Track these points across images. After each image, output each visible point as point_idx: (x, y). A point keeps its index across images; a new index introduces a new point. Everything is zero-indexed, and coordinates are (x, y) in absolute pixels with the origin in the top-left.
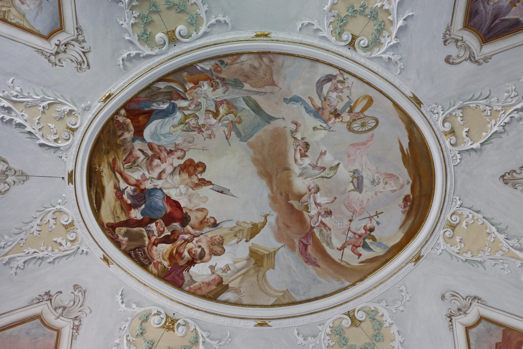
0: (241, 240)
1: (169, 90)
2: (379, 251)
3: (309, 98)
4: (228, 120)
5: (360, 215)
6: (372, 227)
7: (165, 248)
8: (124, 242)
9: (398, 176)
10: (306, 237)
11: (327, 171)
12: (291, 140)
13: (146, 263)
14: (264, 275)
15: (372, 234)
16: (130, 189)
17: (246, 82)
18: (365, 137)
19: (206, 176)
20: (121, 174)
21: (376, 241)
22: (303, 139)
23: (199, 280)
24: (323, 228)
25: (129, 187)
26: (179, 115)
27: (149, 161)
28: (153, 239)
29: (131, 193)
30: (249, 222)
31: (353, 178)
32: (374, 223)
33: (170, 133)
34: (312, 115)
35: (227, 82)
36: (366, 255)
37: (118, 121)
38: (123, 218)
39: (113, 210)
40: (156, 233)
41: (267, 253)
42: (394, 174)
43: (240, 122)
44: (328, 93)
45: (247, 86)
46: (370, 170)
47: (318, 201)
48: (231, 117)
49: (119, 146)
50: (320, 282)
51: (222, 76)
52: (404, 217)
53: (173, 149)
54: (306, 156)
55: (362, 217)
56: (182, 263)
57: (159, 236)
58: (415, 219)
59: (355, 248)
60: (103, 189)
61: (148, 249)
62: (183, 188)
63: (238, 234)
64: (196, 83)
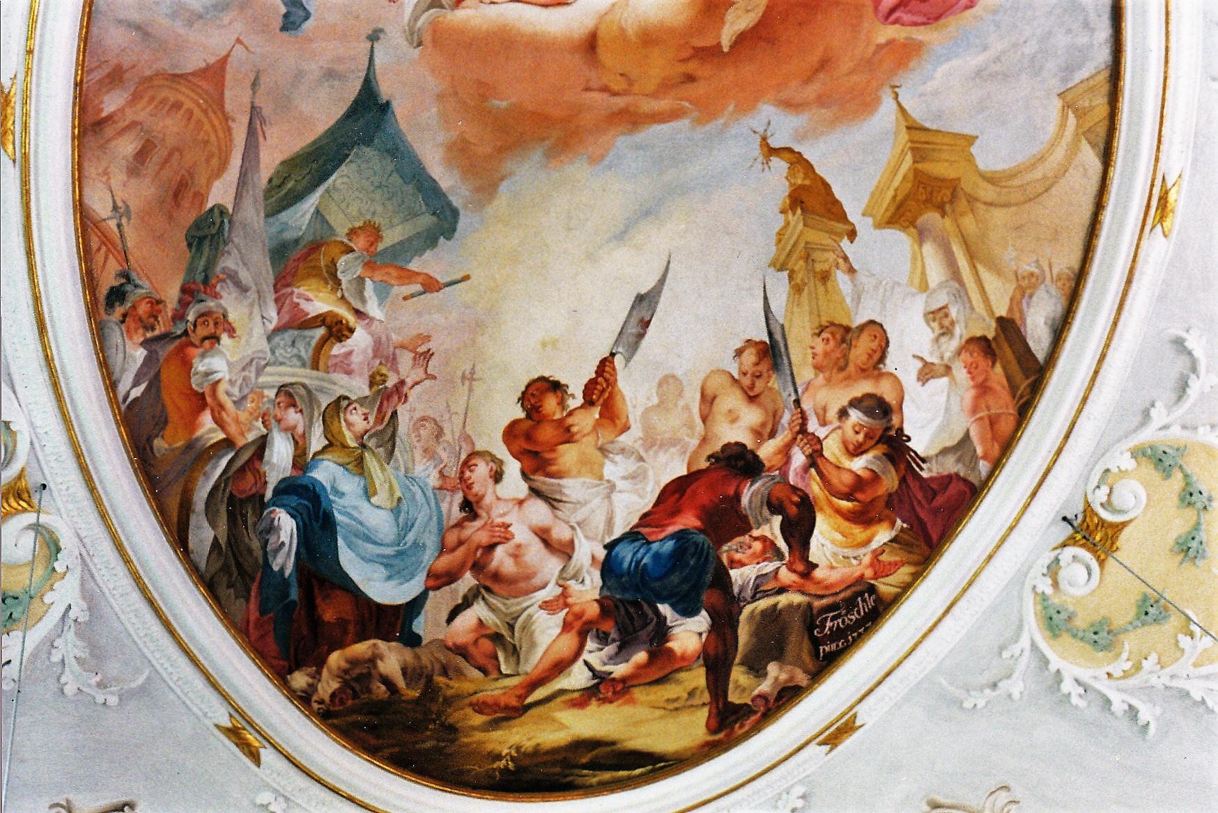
0: (846, 258)
1: (223, 509)
4: (361, 280)
7: (826, 540)
8: (783, 677)
13: (871, 603)
14: (992, 179)
16: (595, 654)
17: (201, 197)
20: (534, 685)
23: (962, 423)
25: (585, 656)
26: (326, 473)
27: (495, 587)
28: (786, 576)
29: (610, 649)
30: (780, 221)
33: (396, 511)
35: (199, 277)
37: (333, 695)
38: (697, 678)
39: (662, 712)
40: (769, 567)
41: (909, 159)
43: (374, 232)
45: (220, 193)
48: (348, 268)
49: (431, 690)
51: (172, 294)
53: (459, 497)
56: (890, 481)
57: (779, 555)
60: (581, 745)
61: (822, 597)
62: (614, 469)
63: (818, 267)
64: (199, 402)
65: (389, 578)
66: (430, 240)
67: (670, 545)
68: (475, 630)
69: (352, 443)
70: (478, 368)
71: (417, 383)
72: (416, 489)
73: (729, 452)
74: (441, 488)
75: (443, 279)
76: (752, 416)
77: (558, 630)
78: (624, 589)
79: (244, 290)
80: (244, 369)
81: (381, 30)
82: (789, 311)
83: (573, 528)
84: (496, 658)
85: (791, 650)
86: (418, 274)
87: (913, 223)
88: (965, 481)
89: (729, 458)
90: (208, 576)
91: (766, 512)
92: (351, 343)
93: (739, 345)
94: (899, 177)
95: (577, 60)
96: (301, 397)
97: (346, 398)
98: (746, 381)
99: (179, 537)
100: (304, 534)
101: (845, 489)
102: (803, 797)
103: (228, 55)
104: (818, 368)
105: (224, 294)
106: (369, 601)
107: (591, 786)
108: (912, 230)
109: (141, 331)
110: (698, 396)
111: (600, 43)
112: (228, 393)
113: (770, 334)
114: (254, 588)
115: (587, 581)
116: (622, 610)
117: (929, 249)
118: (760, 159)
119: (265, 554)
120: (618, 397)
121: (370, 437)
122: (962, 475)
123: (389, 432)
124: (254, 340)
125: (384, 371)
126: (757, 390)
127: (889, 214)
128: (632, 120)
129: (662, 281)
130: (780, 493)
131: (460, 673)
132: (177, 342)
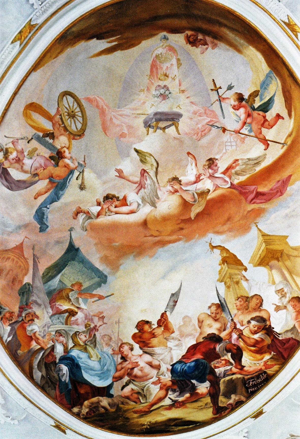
0: (244, 277)
1: (43, 367)
2: (275, 88)
3: (35, 198)
4: (77, 299)
5: (216, 116)
6: (236, 97)
8: (237, 398)
9: (154, 55)
12: (103, 220)
13: (265, 376)
15: (246, 97)
16: (172, 395)
17: (21, 281)
18: (90, 111)
19: (154, 319)
21: (259, 91)
22: (99, 204)
24: (233, 171)
25: (169, 396)
26: (75, 353)
27: (135, 379)
29: (177, 394)
30: (219, 268)
31: (158, 128)
33: (100, 361)
34: (61, 192)
35: (24, 304)
36: (279, 107)
37: (87, 413)
39: (197, 410)
40: (228, 368)
41: (264, 245)
42: (151, 62)
43: (80, 285)
44: (26, 172)
45: (27, 279)
46: (144, 103)
47: (193, 179)
48: (73, 296)
49: (119, 409)
51: (16, 310)
52: (222, 45)
53: (120, 356)
54: (125, 198)
55: (219, 112)
56: (268, 341)
57: (231, 364)
58: (226, 26)
59: (267, 123)
60: (170, 420)
61: (248, 375)
62: (171, 344)
63: (235, 280)
64: (31, 338)
65: (100, 380)
66: (99, 285)
67: (193, 364)
68: (131, 391)
69: (82, 344)
70: (120, 320)
71: (101, 326)
72: (105, 355)
73: (210, 336)
74: (113, 354)
75: (105, 295)
76: (217, 325)
77: (159, 390)
78: (179, 377)
79: (40, 305)
80: (43, 327)
81: (73, 228)
82: (226, 294)
83: (159, 361)
84: (139, 398)
85: (239, 391)
86: (96, 295)
87: (267, 264)
88: (295, 340)
89: (210, 338)
90: (42, 385)
91: (225, 352)
92: (77, 317)
93: (209, 305)
94: (261, 251)
95: (141, 229)
96: (63, 333)
97: (78, 332)
98: (213, 315)
99: (30, 376)
100: (71, 370)
101: (252, 344)
102: (247, 432)
103: (23, 242)
104: (238, 309)
105: (33, 307)
106: (95, 387)
107: (175, 431)
108: (268, 267)
109: (8, 322)
110: (197, 321)
111: (148, 222)
112: (39, 335)
113: (220, 301)
114: (57, 386)
115: (166, 375)
116: (180, 383)
117: (274, 271)
118: (210, 250)
119: (59, 377)
120: (169, 324)
121: (88, 341)
122: (294, 338)
123: (94, 340)
124: (46, 318)
125: (89, 323)
126: (217, 318)
127: (258, 262)
128: (163, 243)
129: (180, 289)
130: (228, 346)
131: (127, 403)
132: (20, 323)
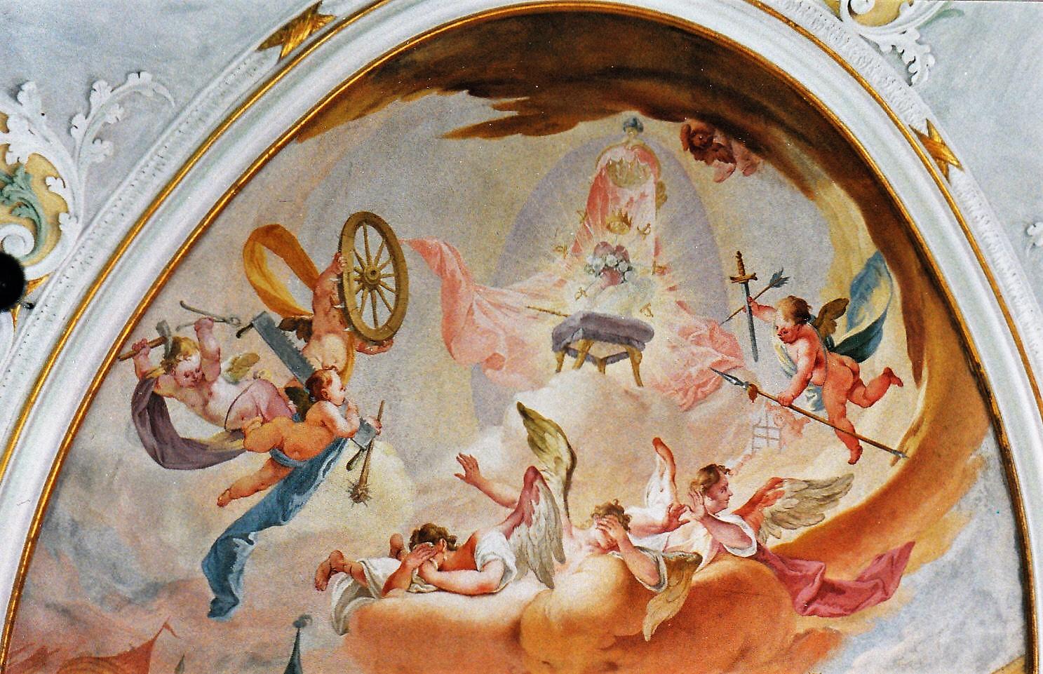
2: (885, 300)
3: (221, 505)
5: (735, 351)
6: (786, 308)
9: (602, 163)
10: (790, 582)
11: (544, 465)
12: (402, 604)
15: (815, 312)
18: (419, 279)
21: (846, 302)
22: (396, 552)
24: (767, 511)
31: (587, 357)
32: (776, 297)
34: (297, 499)
36: (891, 350)
42: (591, 178)
44: (213, 419)
46: (562, 282)
47: (660, 517)
50: (968, 553)
52: (768, 169)
54: (471, 545)
58: (781, 124)
59: (859, 391)
81: (308, 617)
103: (154, 640)
